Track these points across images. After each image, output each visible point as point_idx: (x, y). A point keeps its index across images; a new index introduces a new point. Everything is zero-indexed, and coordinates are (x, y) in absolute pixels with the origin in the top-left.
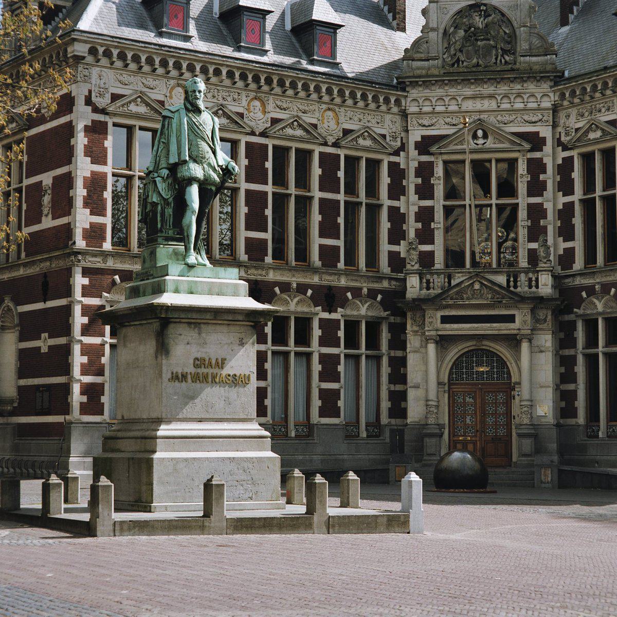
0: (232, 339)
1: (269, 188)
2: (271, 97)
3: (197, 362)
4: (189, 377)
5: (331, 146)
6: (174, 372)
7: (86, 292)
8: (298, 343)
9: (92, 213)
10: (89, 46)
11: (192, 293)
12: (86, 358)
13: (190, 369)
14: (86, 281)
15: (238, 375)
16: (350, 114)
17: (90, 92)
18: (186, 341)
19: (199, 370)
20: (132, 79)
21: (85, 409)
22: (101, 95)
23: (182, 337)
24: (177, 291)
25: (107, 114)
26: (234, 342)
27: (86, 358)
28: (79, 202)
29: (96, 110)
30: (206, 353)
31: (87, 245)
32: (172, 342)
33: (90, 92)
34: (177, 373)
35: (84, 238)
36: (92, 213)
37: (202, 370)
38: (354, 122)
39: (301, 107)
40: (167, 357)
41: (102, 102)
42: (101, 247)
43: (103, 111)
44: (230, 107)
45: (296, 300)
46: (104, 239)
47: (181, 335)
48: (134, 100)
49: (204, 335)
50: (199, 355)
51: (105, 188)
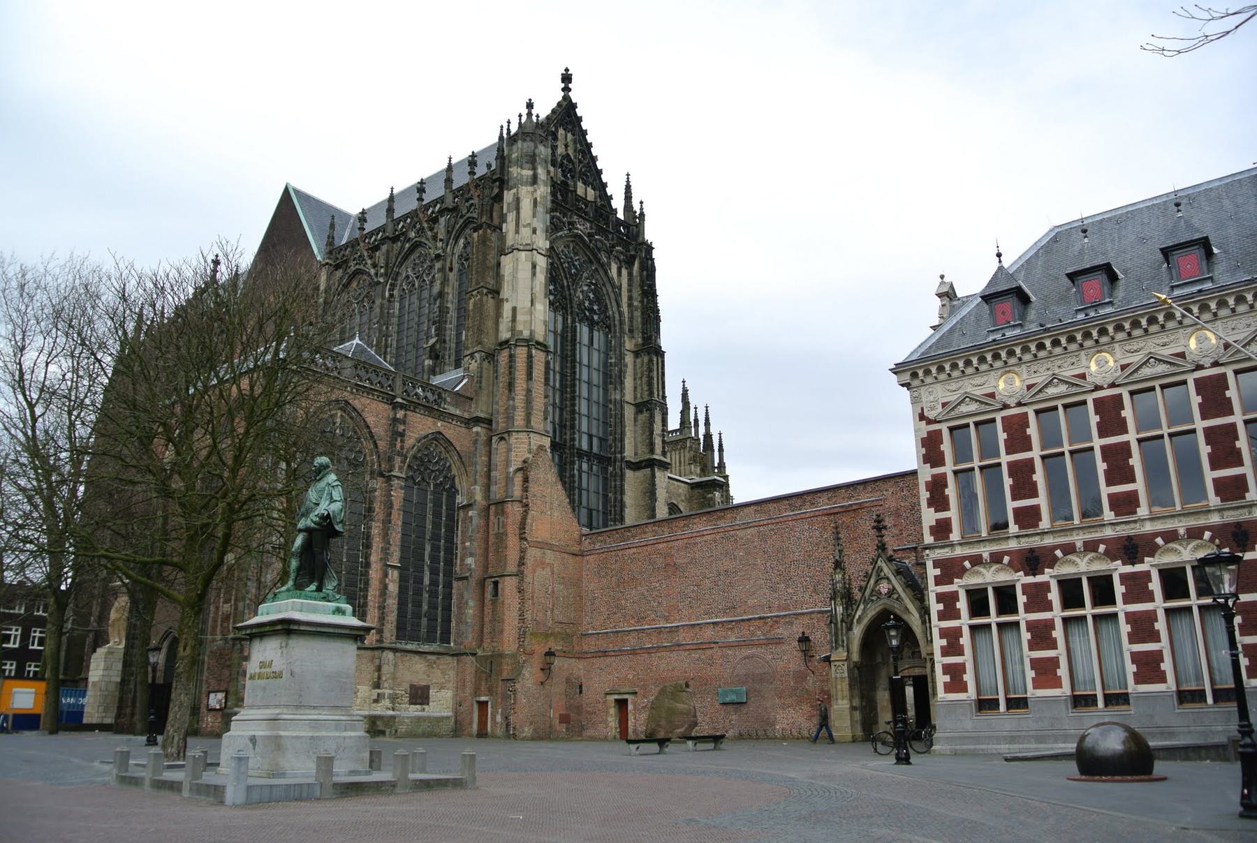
1: (1165, 431)
2: (1116, 345)
5: (1209, 368)
7: (939, 581)
8: (1001, 612)
9: (936, 511)
10: (909, 373)
12: (945, 640)
14: (938, 572)
16: (1231, 324)
17: (922, 409)
20: (961, 383)
21: (949, 688)
22: (932, 409)
25: (940, 422)
27: (945, 640)
28: (924, 503)
29: (929, 422)
31: (935, 540)
33: (922, 409)
35: (932, 534)
36: (936, 511)
38: (1239, 331)
39: (1157, 342)
41: (931, 415)
42: (948, 538)
43: (935, 422)
44: (1064, 374)
45: (1191, 546)
46: (951, 531)
48: (962, 401)
51: (946, 486)
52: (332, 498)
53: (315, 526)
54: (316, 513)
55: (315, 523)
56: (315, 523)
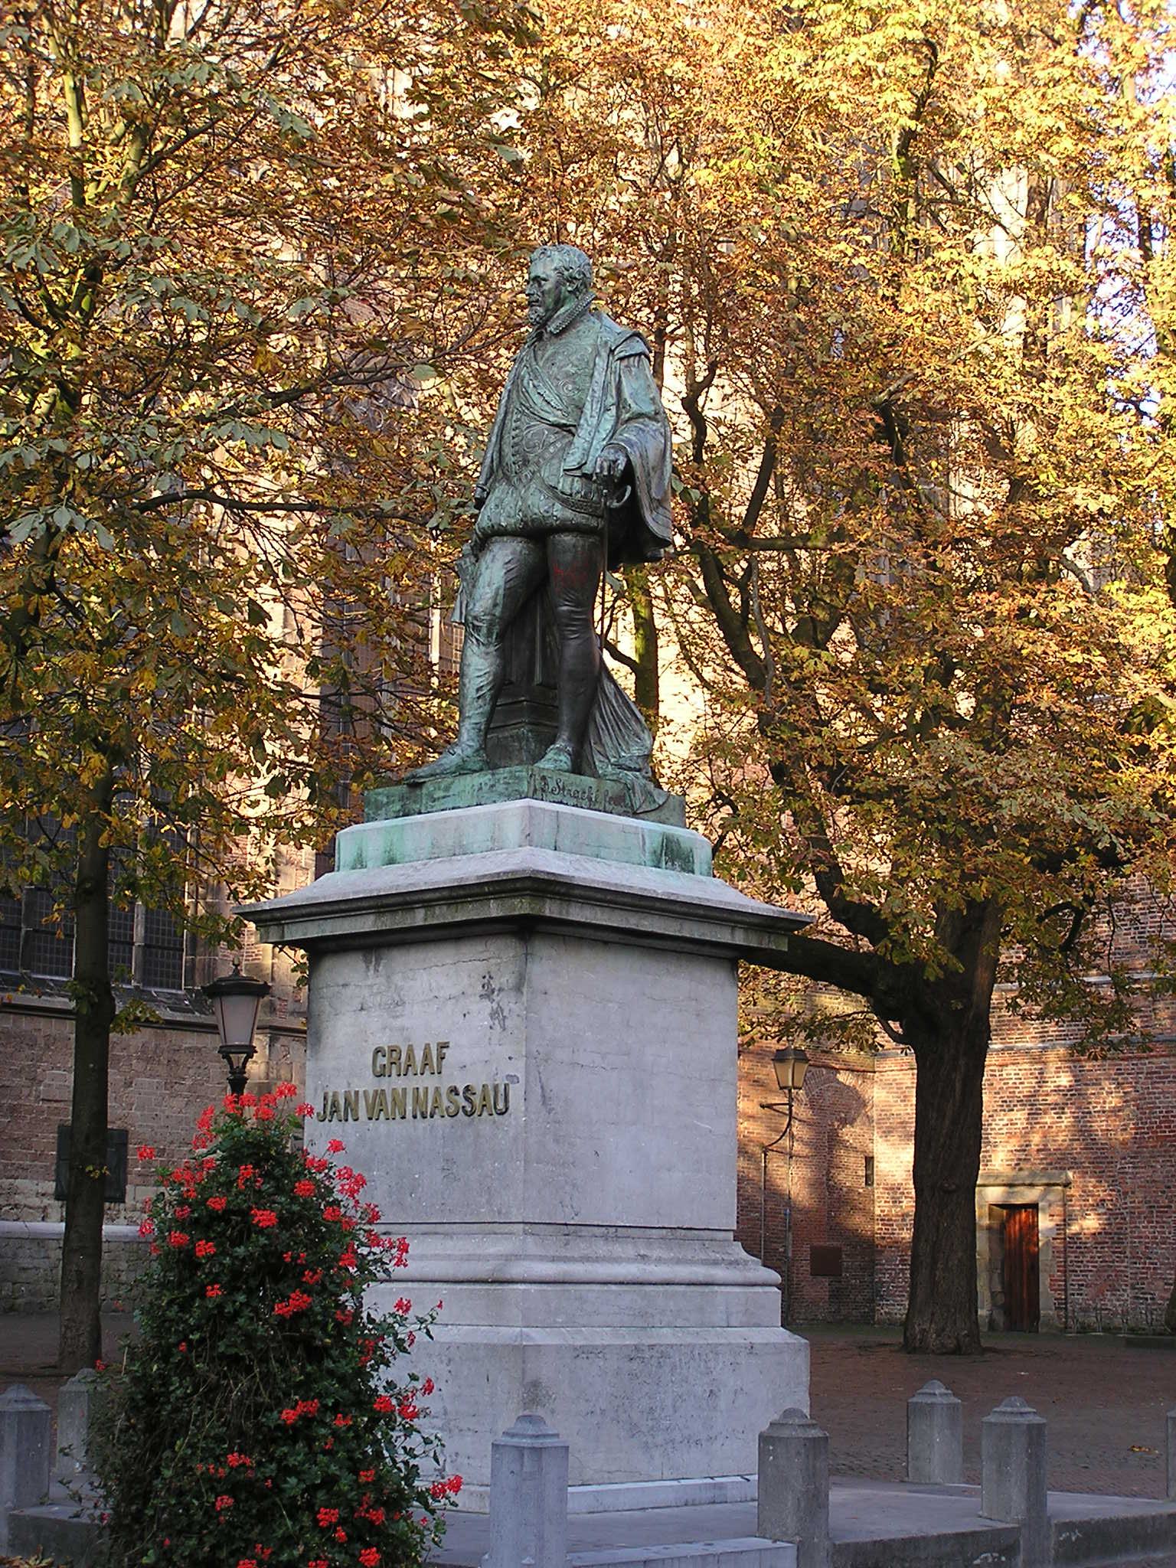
0: (466, 981)
3: (382, 1061)
4: (362, 1103)
6: (331, 1094)
11: (391, 861)
13: (366, 1084)
15: (479, 1090)
18: (356, 1004)
19: (385, 1084)
23: (349, 991)
24: (359, 863)
26: (469, 991)
30: (403, 1029)
32: (328, 1009)
34: (335, 1094)
37: (394, 1083)
40: (317, 1052)
47: (345, 985)
49: (397, 979)
50: (385, 1043)
52: (620, 403)
53: (569, 514)
54: (572, 462)
55: (566, 501)
56: (566, 501)
